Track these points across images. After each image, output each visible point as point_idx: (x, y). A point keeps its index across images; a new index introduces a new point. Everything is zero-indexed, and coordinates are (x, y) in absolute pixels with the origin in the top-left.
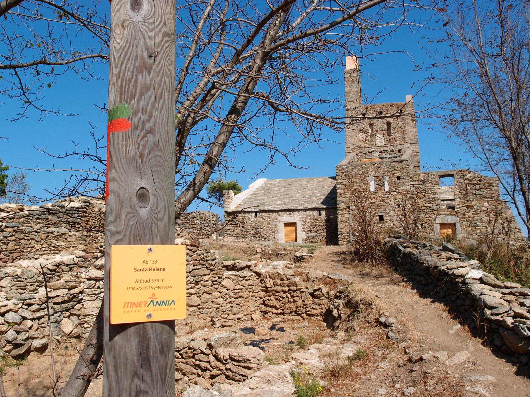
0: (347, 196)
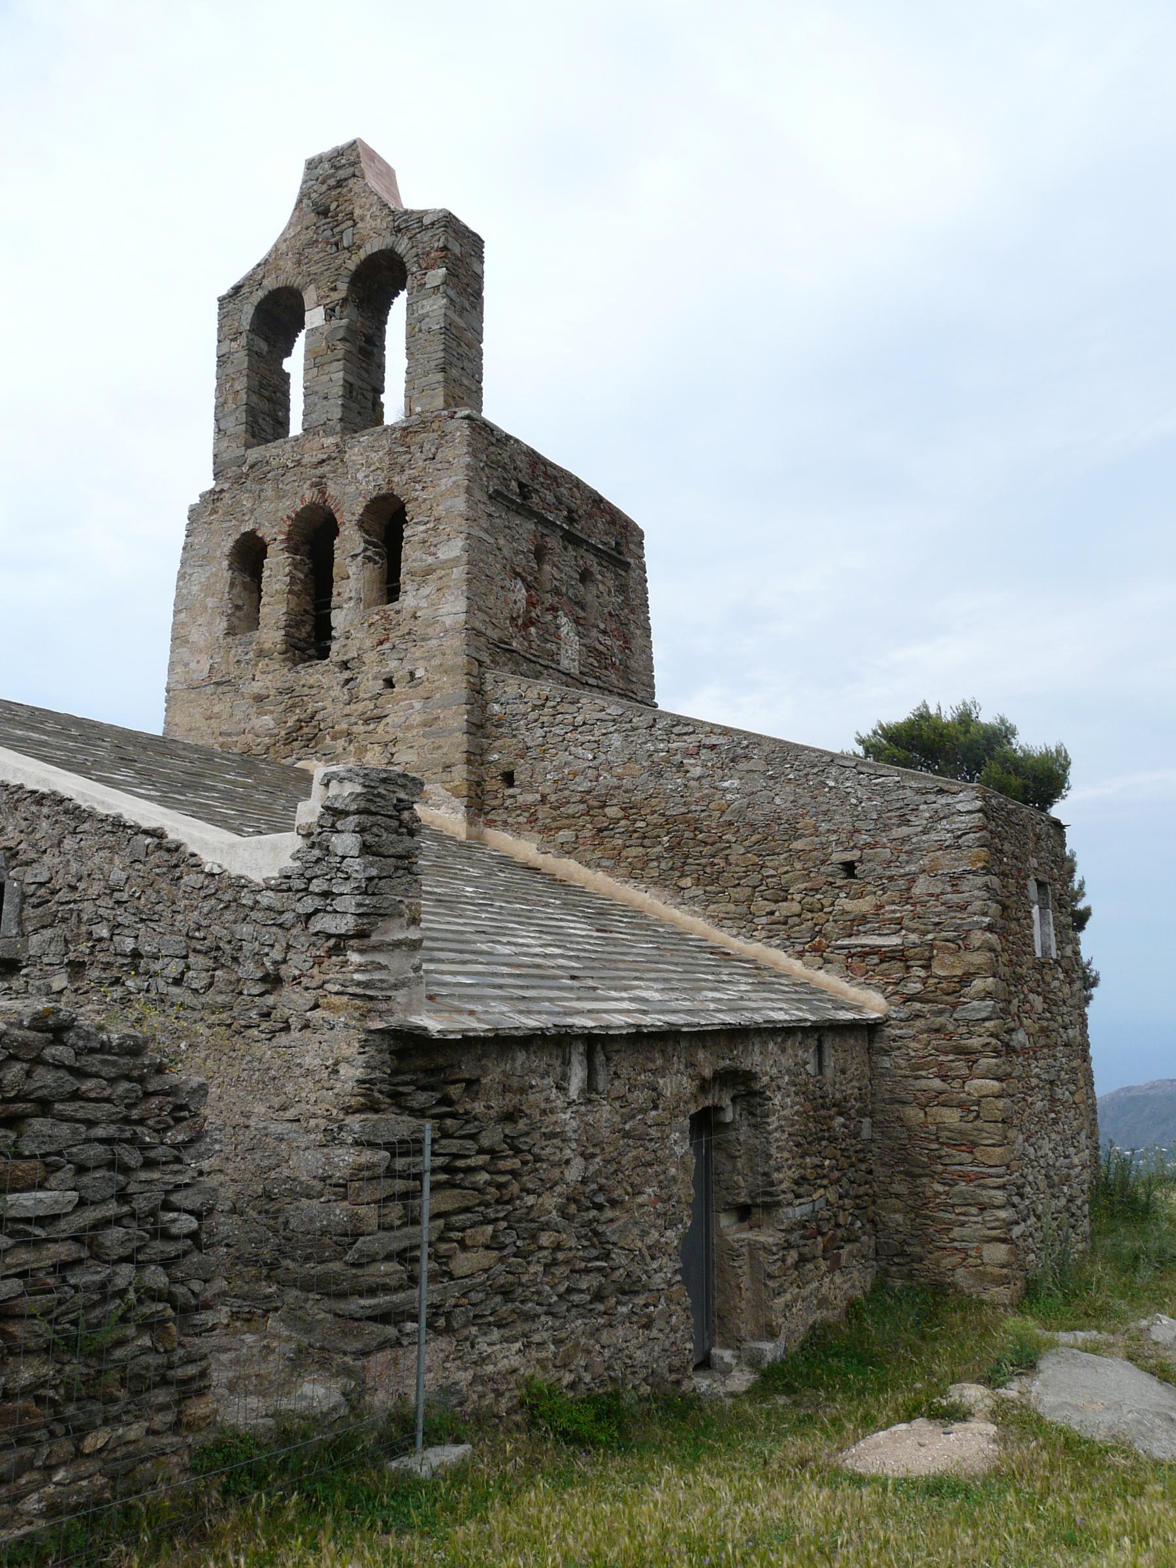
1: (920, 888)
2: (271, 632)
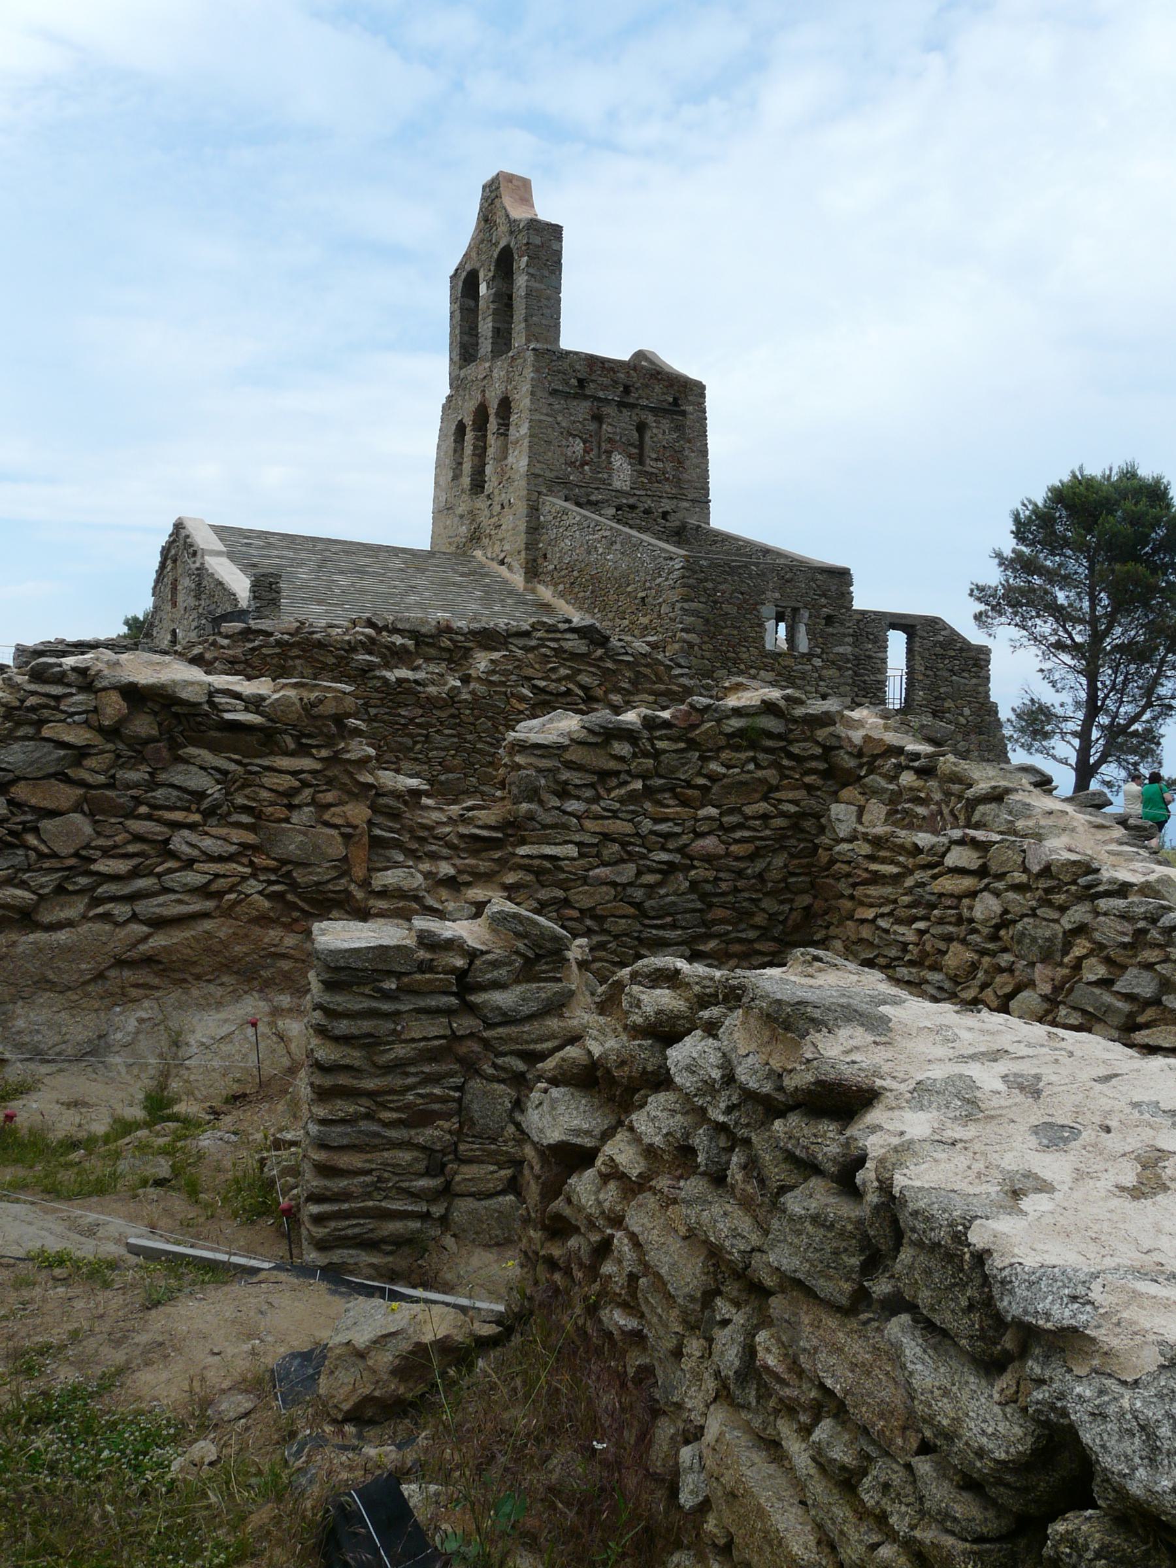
0: (707, 654)
1: (664, 609)
2: (466, 481)
